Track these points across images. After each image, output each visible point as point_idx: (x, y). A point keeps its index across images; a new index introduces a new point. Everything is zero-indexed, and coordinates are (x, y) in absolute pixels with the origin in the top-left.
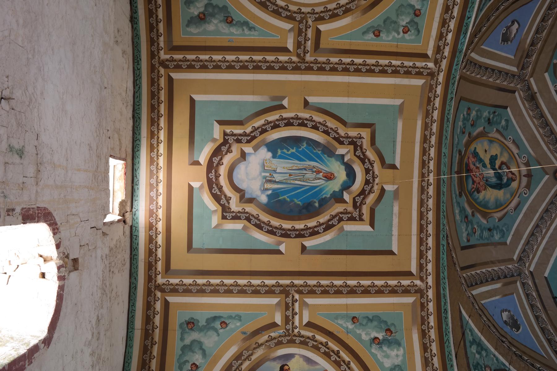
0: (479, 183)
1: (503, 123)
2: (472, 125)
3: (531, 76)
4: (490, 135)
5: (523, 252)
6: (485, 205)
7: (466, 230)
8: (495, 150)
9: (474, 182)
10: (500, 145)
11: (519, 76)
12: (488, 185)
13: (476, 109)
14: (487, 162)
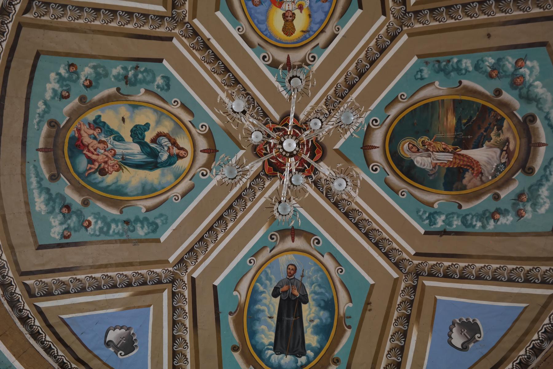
0: (106, 162)
1: (159, 81)
2: (87, 87)
3: (194, 17)
4: (130, 98)
5: (189, 252)
6: (119, 190)
7: (61, 224)
8: (143, 117)
9: (91, 161)
10: (155, 111)
11: (173, 18)
12: (126, 164)
13: (91, 64)
14: (126, 134)
